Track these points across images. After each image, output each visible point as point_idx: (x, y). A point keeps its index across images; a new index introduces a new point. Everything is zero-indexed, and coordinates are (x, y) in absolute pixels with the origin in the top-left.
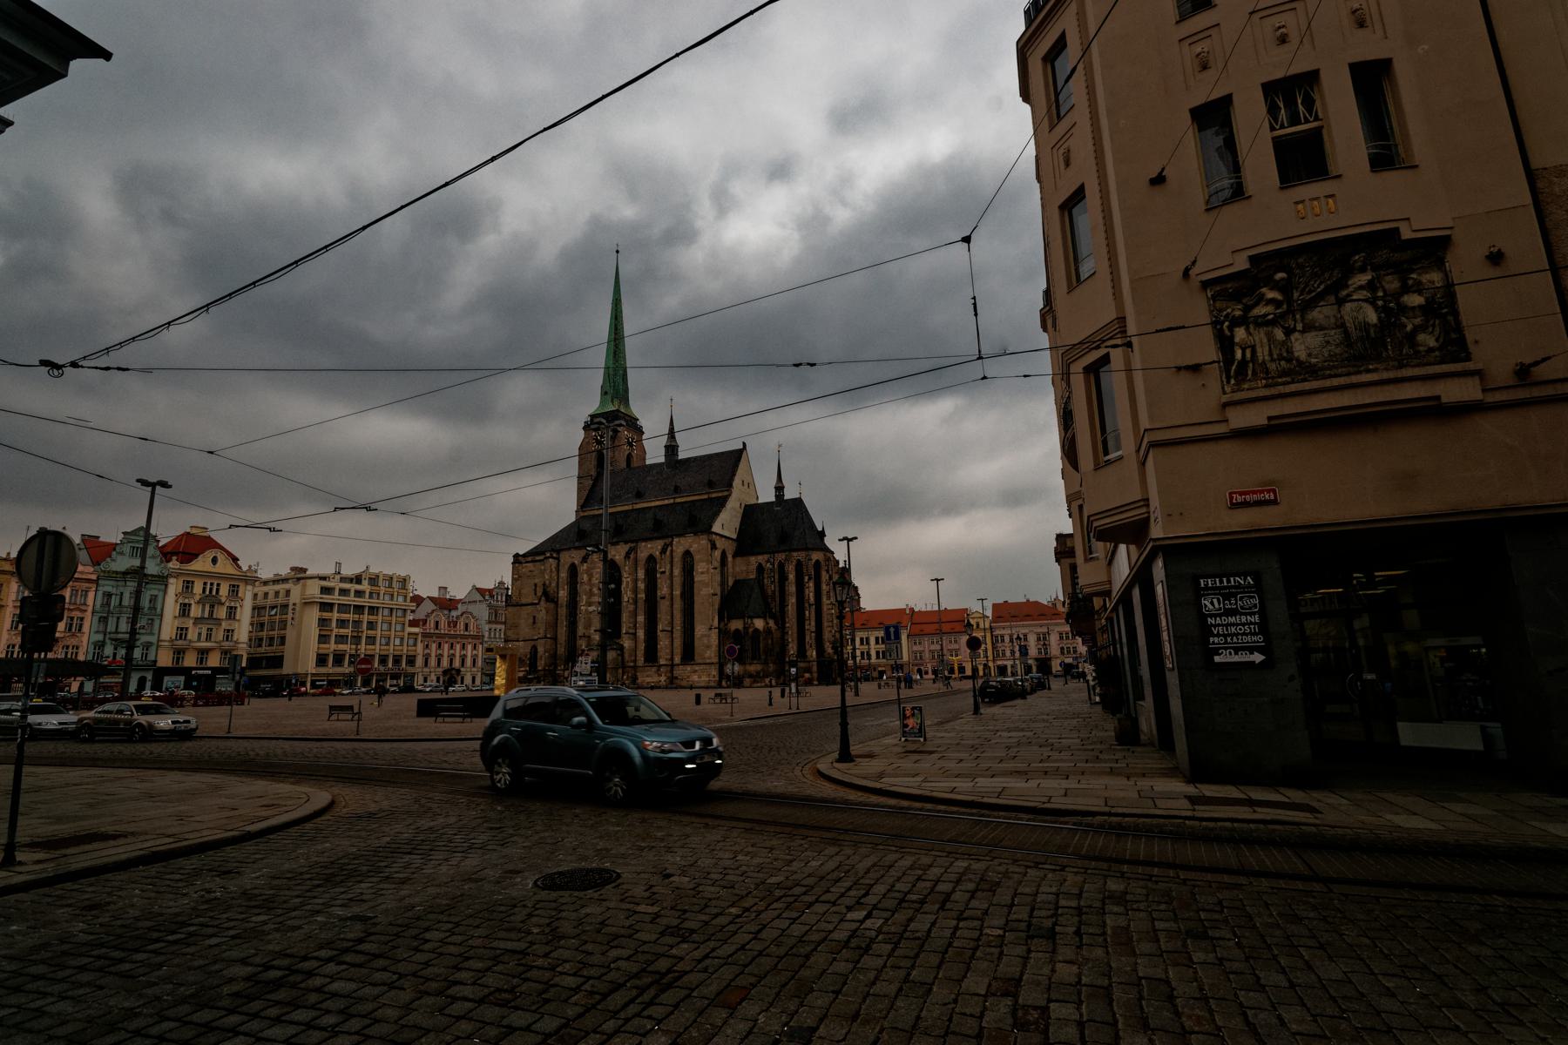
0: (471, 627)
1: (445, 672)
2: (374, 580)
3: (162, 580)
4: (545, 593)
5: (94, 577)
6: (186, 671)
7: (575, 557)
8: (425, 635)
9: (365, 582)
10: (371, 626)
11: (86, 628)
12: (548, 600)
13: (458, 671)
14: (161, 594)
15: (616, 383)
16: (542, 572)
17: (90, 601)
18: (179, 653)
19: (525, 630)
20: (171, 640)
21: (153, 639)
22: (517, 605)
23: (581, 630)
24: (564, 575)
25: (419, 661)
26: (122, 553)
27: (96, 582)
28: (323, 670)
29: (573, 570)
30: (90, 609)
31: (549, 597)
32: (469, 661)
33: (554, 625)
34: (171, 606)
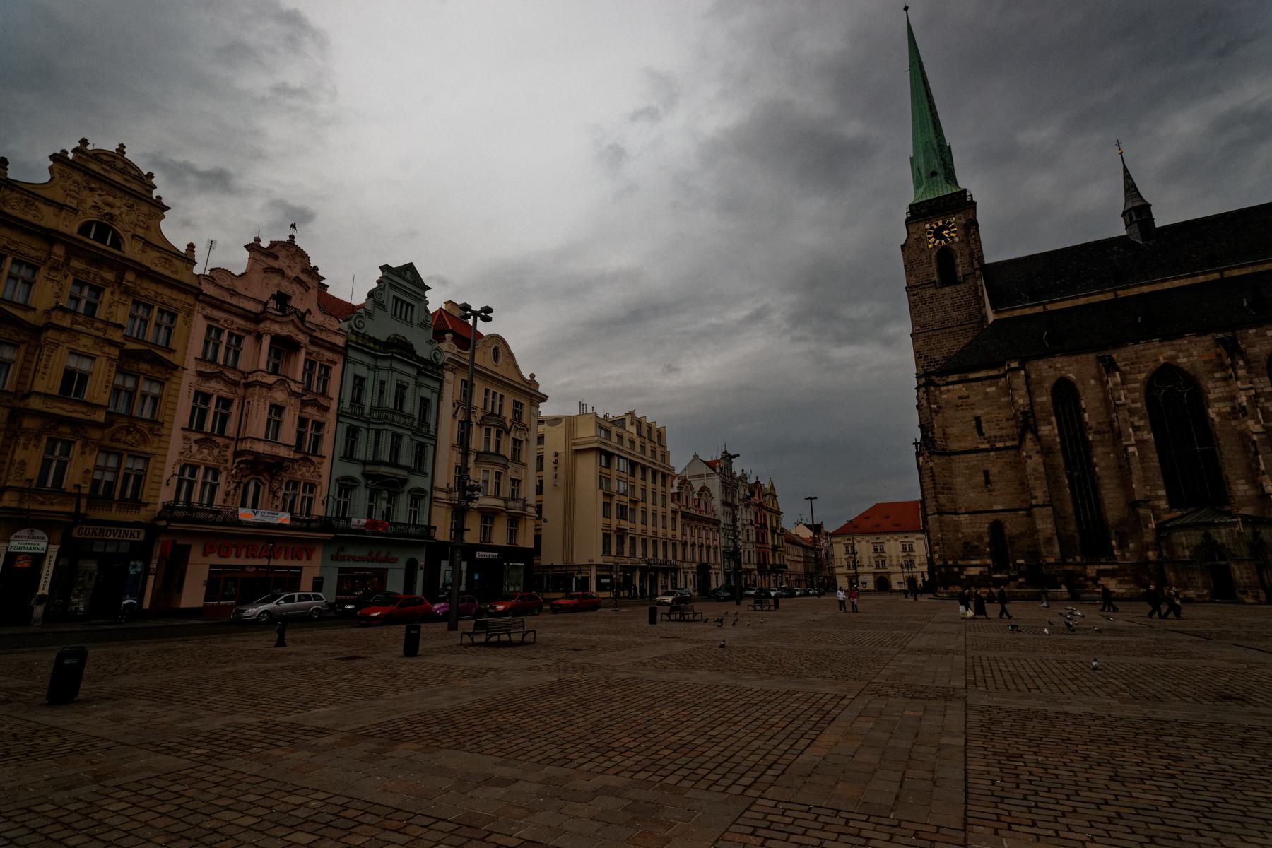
3: (431, 370)
5: (340, 341)
6: (470, 550)
11: (326, 448)
14: (435, 396)
15: (935, 157)
17: (333, 390)
18: (460, 513)
21: (423, 483)
28: (609, 561)
30: (334, 406)
34: (447, 430)
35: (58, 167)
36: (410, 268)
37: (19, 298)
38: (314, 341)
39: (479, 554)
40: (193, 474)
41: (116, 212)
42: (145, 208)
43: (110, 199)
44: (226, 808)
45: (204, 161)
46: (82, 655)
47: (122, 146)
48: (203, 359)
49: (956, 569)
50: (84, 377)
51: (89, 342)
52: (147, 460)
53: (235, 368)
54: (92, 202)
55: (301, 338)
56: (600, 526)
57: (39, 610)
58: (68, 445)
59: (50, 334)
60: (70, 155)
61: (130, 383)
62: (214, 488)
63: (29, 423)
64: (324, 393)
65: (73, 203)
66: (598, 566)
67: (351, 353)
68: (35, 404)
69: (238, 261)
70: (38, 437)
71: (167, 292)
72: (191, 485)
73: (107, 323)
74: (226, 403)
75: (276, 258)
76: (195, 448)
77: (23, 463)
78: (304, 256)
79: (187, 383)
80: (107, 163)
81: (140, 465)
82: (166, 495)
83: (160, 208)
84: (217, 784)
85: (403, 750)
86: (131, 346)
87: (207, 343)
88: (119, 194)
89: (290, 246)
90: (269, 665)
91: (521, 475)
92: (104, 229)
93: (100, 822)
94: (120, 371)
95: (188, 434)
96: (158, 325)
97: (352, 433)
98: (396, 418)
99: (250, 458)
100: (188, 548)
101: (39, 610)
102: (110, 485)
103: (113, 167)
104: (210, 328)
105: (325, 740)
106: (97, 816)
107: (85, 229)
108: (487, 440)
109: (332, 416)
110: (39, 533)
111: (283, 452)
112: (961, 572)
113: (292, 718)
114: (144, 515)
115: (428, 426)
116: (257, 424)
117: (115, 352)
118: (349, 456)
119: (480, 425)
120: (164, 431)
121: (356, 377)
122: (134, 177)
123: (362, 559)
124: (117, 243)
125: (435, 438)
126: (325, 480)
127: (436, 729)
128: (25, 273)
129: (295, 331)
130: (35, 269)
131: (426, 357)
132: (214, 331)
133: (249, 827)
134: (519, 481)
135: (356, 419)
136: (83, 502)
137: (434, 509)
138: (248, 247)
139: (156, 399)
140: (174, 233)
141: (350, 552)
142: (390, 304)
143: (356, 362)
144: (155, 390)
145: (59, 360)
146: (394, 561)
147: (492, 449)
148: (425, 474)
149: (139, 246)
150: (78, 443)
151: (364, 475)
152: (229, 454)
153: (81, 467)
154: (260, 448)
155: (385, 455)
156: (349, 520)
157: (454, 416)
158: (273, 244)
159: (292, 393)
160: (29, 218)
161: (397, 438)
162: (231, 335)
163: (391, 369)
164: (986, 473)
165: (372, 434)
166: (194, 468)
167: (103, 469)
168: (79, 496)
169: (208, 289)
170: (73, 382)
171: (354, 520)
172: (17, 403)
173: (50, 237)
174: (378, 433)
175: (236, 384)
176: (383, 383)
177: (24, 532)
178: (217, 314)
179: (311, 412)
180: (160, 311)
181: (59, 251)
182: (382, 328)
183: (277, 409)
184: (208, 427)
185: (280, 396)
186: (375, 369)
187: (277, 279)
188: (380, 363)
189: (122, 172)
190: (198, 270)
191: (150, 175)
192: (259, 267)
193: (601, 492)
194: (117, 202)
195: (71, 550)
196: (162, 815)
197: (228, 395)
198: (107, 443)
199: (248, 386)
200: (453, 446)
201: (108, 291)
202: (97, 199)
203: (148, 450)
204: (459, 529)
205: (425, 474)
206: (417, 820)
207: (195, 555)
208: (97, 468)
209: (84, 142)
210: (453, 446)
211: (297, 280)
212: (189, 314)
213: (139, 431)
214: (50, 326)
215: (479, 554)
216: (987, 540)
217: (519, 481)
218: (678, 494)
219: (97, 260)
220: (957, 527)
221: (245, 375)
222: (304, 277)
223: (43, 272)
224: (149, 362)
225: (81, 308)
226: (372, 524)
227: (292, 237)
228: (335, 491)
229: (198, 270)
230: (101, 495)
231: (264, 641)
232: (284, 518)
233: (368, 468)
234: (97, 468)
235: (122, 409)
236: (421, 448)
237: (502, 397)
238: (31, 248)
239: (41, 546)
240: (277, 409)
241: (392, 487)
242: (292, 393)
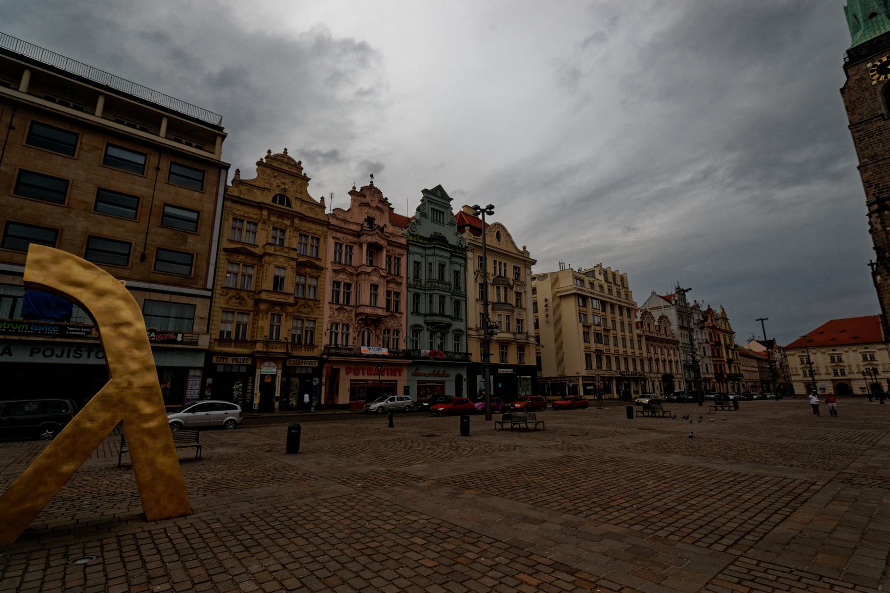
3: (458, 252)
5: (403, 241)
11: (403, 308)
14: (463, 268)
17: (403, 273)
18: (485, 344)
28: (592, 373)
30: (404, 281)
34: (472, 291)
35: (261, 167)
36: (439, 188)
37: (251, 242)
38: (390, 243)
39: (500, 371)
40: (337, 329)
41: (287, 187)
42: (299, 182)
43: (283, 180)
44: (376, 518)
45: (325, 148)
46: (299, 428)
47: (286, 149)
48: (334, 263)
50: (283, 279)
51: (282, 260)
52: (315, 321)
53: (350, 265)
54: (276, 184)
55: (383, 243)
56: (583, 349)
57: (277, 404)
58: (280, 316)
59: (266, 258)
60: (264, 161)
61: (302, 280)
62: (347, 335)
63: (263, 306)
64: (398, 275)
65: (267, 186)
66: (583, 377)
67: (411, 248)
68: (264, 296)
69: (345, 202)
70: (267, 313)
71: (314, 226)
72: (336, 334)
73: (289, 248)
74: (348, 286)
75: (365, 196)
76: (336, 313)
77: (262, 327)
78: (379, 192)
79: (328, 277)
80: (280, 160)
81: (311, 325)
82: (325, 341)
83: (306, 179)
84: (370, 504)
85: (468, 494)
86: (301, 259)
87: (335, 252)
88: (287, 176)
89: (371, 189)
90: (387, 438)
91: (523, 316)
92: (282, 198)
93: (318, 518)
94: (299, 274)
95: (332, 306)
96: (312, 246)
97: (416, 297)
99: (364, 317)
100: (339, 370)
101: (277, 404)
102: (300, 337)
103: (283, 162)
104: (336, 244)
105: (422, 484)
106: (316, 514)
107: (274, 200)
108: (499, 294)
109: (404, 287)
110: (273, 364)
111: (380, 312)
113: (403, 469)
114: (316, 353)
115: (460, 288)
116: (365, 298)
117: (294, 264)
118: (416, 312)
119: (493, 285)
120: (321, 305)
121: (415, 262)
122: (292, 165)
123: (430, 375)
124: (289, 204)
125: (465, 296)
126: (404, 328)
127: (487, 483)
128: (252, 227)
129: (379, 239)
130: (256, 224)
131: (455, 244)
133: (390, 531)
134: (522, 321)
136: (289, 346)
137: (469, 342)
138: (351, 193)
139: (315, 288)
140: (314, 192)
141: (423, 370)
142: (430, 214)
144: (314, 282)
145: (271, 272)
146: (448, 376)
147: (502, 300)
148: (462, 320)
149: (299, 203)
150: (284, 315)
151: (427, 323)
152: (353, 315)
153: (287, 328)
154: (368, 311)
155: (436, 310)
156: (420, 351)
157: (476, 280)
158: (362, 189)
159: (381, 276)
160: (252, 199)
161: (442, 298)
162: (347, 246)
163: (434, 255)
165: (428, 296)
166: (337, 325)
167: (295, 328)
168: (287, 343)
169: (333, 221)
170: (278, 282)
171: (423, 351)
172: (257, 297)
173: (260, 206)
174: (431, 296)
175: (352, 274)
176: (430, 264)
177: (266, 364)
178: (339, 235)
179: (392, 286)
180: (312, 238)
181: (265, 213)
182: (427, 230)
183: (375, 287)
184: (341, 301)
185: (375, 279)
186: (425, 256)
187: (366, 209)
188: (428, 252)
189: (288, 164)
190: (327, 211)
191: (300, 163)
192: (357, 204)
193: (581, 325)
194: (286, 181)
195: (288, 372)
196: (346, 518)
197: (348, 281)
198: (296, 314)
199: (358, 275)
200: (477, 300)
201: (288, 230)
202: (278, 181)
203: (315, 316)
204: (486, 355)
205: (462, 320)
206: (483, 539)
207: (343, 373)
208: (294, 328)
209: (269, 152)
210: (477, 300)
211: (377, 208)
212: (326, 237)
213: (309, 306)
214: (265, 254)
215: (500, 371)
217: (522, 321)
218: (642, 322)
219: (281, 215)
221: (356, 268)
223: (260, 225)
224: (309, 267)
225: (278, 242)
226: (433, 353)
227: (372, 182)
228: (410, 333)
229: (327, 211)
230: (296, 342)
231: (382, 423)
232: (385, 351)
233: (428, 318)
234: (294, 328)
235: (300, 295)
236: (457, 304)
237: (505, 264)
238: (253, 213)
239: (273, 371)
240: (375, 287)
242: (381, 276)
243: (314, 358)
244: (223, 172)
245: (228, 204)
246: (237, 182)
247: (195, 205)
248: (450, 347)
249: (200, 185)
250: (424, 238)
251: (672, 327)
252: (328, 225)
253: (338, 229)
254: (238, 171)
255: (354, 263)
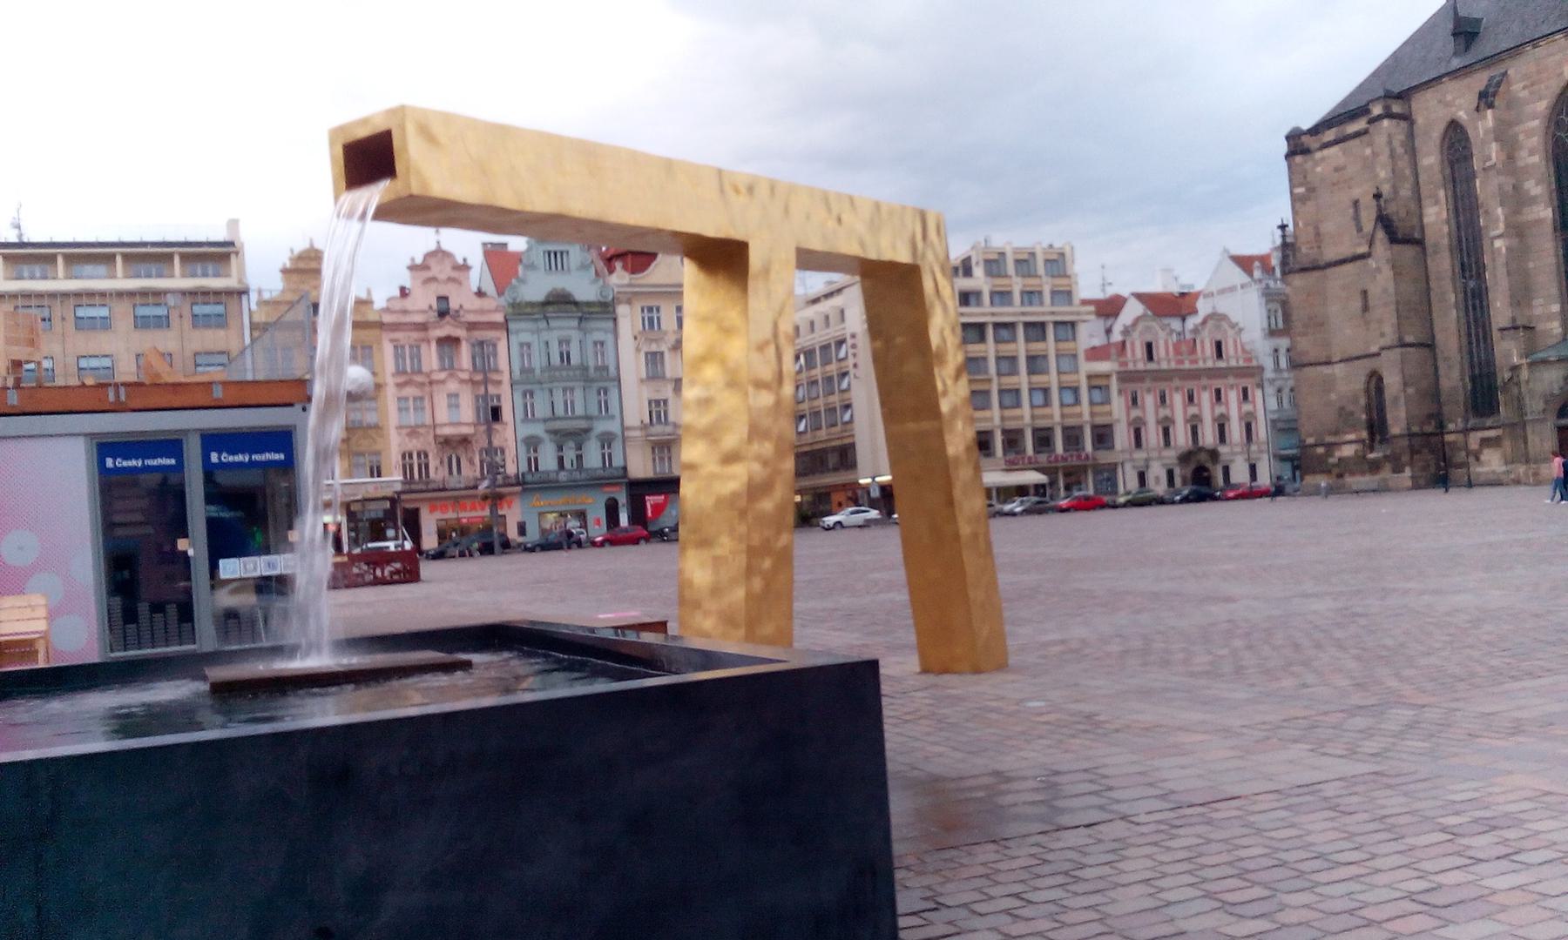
0: (1229, 349)
1: (1185, 458)
2: (994, 265)
3: (606, 309)
4: (1384, 221)
5: (499, 318)
7: (1458, 101)
8: (1126, 377)
9: (978, 271)
10: (1036, 363)
12: (1394, 238)
13: (1214, 455)
14: (609, 338)
16: (1369, 165)
17: (503, 363)
19: (1346, 334)
20: (644, 427)
21: (614, 427)
22: (1315, 267)
23: (1500, 311)
24: (1431, 160)
25: (1122, 437)
26: (531, 267)
27: (505, 326)
29: (1456, 139)
30: (506, 378)
31: (1398, 231)
32: (1235, 431)
33: (1418, 307)
38: (472, 326)
48: (400, 372)
49: (1320, 450)
53: (420, 372)
55: (460, 333)
98: (564, 373)
112: (1329, 454)
121: (522, 345)
126: (511, 443)
132: (398, 348)
135: (527, 383)
143: (517, 332)
148: (613, 417)
151: (547, 431)
152: (431, 439)
154: (447, 431)
157: (638, 350)
159: (462, 381)
164: (1365, 293)
165: (547, 393)
169: (387, 319)
175: (422, 384)
185: (453, 386)
186: (538, 331)
199: (431, 383)
200: (642, 381)
205: (613, 417)
211: (450, 280)
212: (380, 342)
216: (1363, 401)
218: (1124, 343)
220: (1328, 385)
221: (428, 375)
222: (455, 274)
228: (522, 449)
240: (453, 396)
241: (579, 436)
242: (462, 381)
243: (384, 498)
244: (244, 298)
245: (256, 334)
246: (262, 303)
247: (221, 346)
248: (593, 459)
249: (221, 322)
250: (532, 304)
251: (1245, 337)
252: (380, 325)
253: (395, 327)
254: (260, 292)
255: (425, 369)
